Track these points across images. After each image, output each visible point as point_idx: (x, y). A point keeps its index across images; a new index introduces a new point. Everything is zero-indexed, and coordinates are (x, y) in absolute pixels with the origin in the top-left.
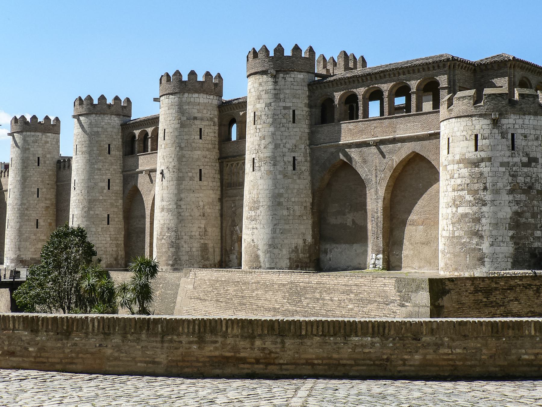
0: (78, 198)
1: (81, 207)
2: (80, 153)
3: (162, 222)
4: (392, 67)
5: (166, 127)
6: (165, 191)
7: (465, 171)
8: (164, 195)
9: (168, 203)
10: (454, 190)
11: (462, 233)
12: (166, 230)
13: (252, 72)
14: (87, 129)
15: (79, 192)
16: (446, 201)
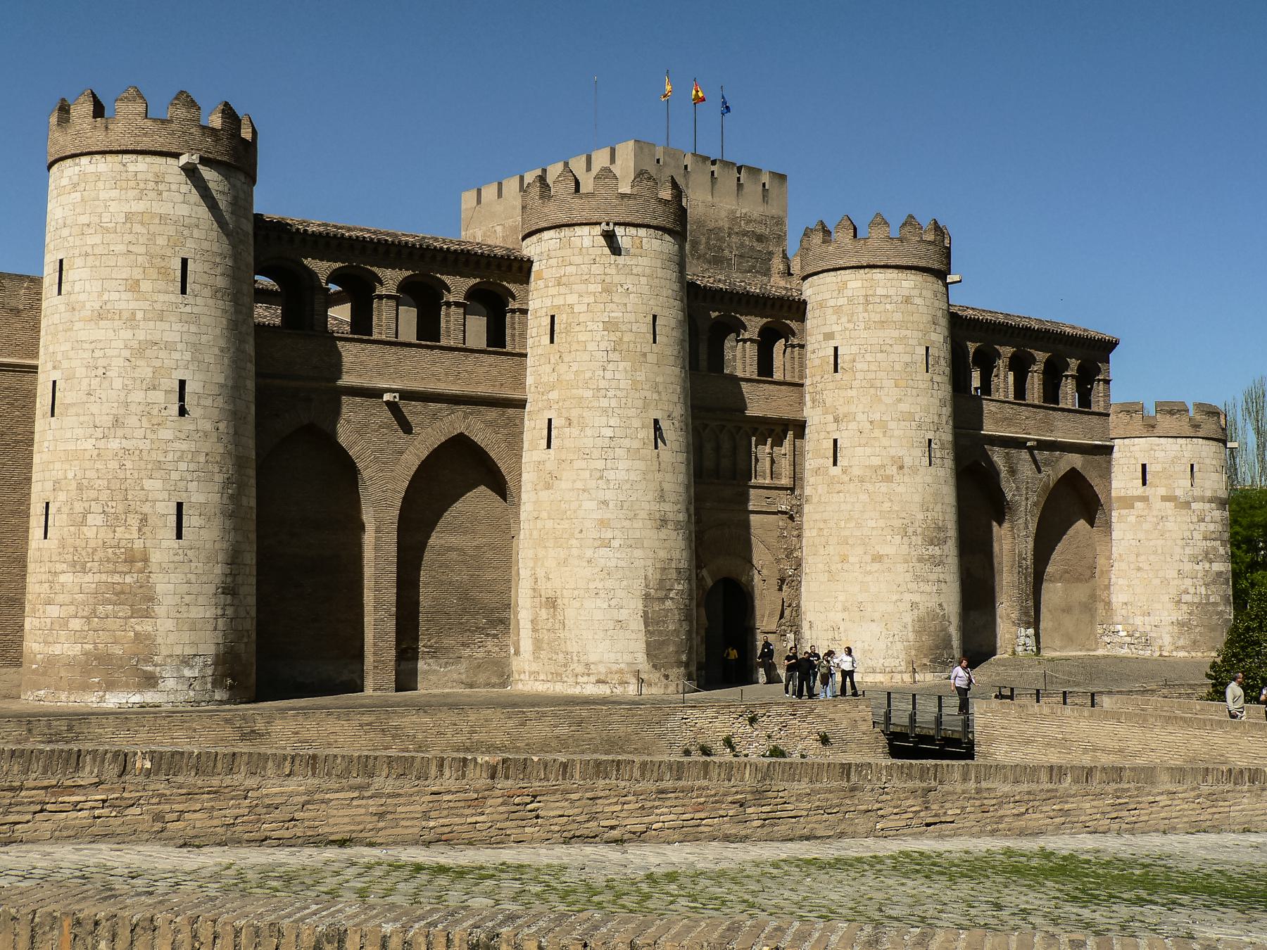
0: (207, 446)
1: (219, 478)
2: (207, 292)
3: (662, 554)
4: (1049, 326)
5: (656, 310)
6: (669, 477)
7: (1217, 514)
8: (666, 486)
9: (676, 508)
10: (1205, 539)
11: (1218, 599)
12: (674, 576)
13: (921, 264)
14: (227, 216)
15: (208, 426)
16: (1188, 551)
